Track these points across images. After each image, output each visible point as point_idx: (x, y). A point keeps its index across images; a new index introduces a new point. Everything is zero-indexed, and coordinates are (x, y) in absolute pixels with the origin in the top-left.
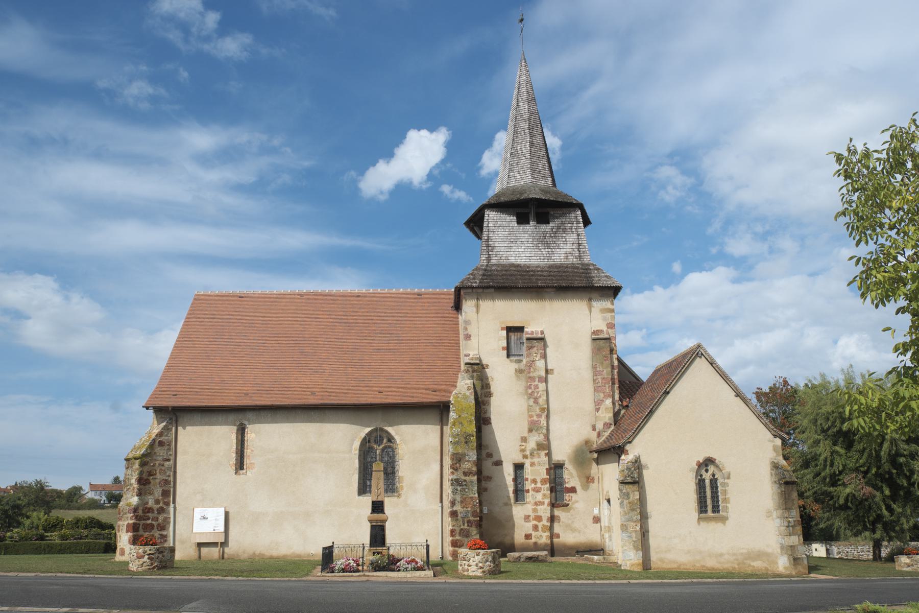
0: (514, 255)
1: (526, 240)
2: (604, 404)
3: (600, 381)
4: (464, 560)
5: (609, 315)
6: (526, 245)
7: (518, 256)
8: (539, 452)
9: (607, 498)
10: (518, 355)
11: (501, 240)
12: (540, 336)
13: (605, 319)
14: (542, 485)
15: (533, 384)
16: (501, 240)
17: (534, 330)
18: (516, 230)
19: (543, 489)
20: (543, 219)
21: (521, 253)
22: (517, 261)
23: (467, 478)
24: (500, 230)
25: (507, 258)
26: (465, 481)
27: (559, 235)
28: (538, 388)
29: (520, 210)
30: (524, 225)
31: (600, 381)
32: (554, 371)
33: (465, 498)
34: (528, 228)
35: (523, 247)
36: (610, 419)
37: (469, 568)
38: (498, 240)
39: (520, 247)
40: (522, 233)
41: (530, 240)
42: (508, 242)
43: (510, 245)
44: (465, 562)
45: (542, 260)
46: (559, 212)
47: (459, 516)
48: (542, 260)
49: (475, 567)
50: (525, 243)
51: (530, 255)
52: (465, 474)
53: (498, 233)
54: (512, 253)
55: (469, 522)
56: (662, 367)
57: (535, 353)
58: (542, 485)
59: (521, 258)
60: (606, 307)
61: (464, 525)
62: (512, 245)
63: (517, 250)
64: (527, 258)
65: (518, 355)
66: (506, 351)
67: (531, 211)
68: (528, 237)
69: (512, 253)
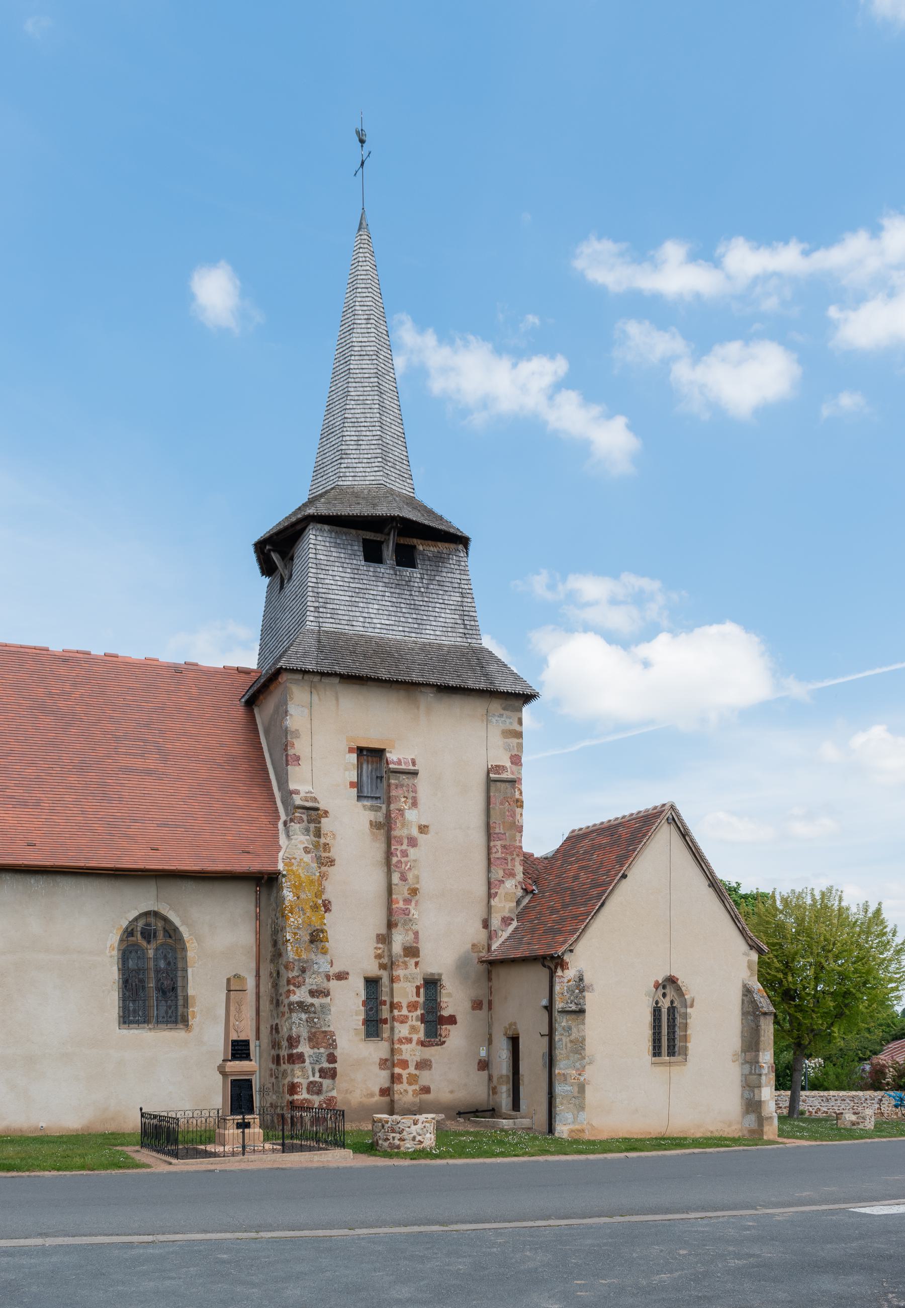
0: (361, 619)
1: (381, 593)
2: (502, 885)
3: (500, 850)
4: (393, 1131)
5: (514, 741)
6: (381, 603)
7: (367, 620)
8: (407, 959)
9: (510, 1033)
10: (372, 798)
11: (339, 588)
12: (411, 767)
13: (508, 748)
14: (409, 1011)
15: (399, 848)
16: (339, 588)
17: (401, 757)
18: (362, 572)
19: (410, 1018)
20: (406, 558)
21: (372, 616)
22: (366, 629)
23: (315, 1001)
24: (336, 569)
25: (350, 623)
26: (312, 1005)
27: (433, 591)
28: (407, 856)
29: (370, 536)
30: (376, 565)
31: (500, 850)
32: (431, 828)
33: (315, 1033)
34: (383, 571)
35: (376, 607)
36: (510, 911)
37: (402, 1143)
38: (334, 587)
39: (371, 606)
40: (373, 579)
41: (387, 594)
42: (350, 594)
43: (353, 599)
44: (394, 1135)
45: (407, 634)
46: (432, 549)
47: (307, 1061)
48: (407, 634)
49: (412, 1142)
50: (379, 598)
51: (387, 622)
52: (312, 993)
53: (334, 573)
54: (358, 614)
55: (321, 1071)
56: (592, 832)
57: (404, 797)
58: (409, 1011)
59: (373, 625)
60: (511, 728)
61: (314, 1076)
62: (357, 600)
63: (366, 610)
64: (384, 627)
65: (372, 798)
66: (356, 789)
67: (387, 541)
68: (383, 589)
69: (358, 614)
